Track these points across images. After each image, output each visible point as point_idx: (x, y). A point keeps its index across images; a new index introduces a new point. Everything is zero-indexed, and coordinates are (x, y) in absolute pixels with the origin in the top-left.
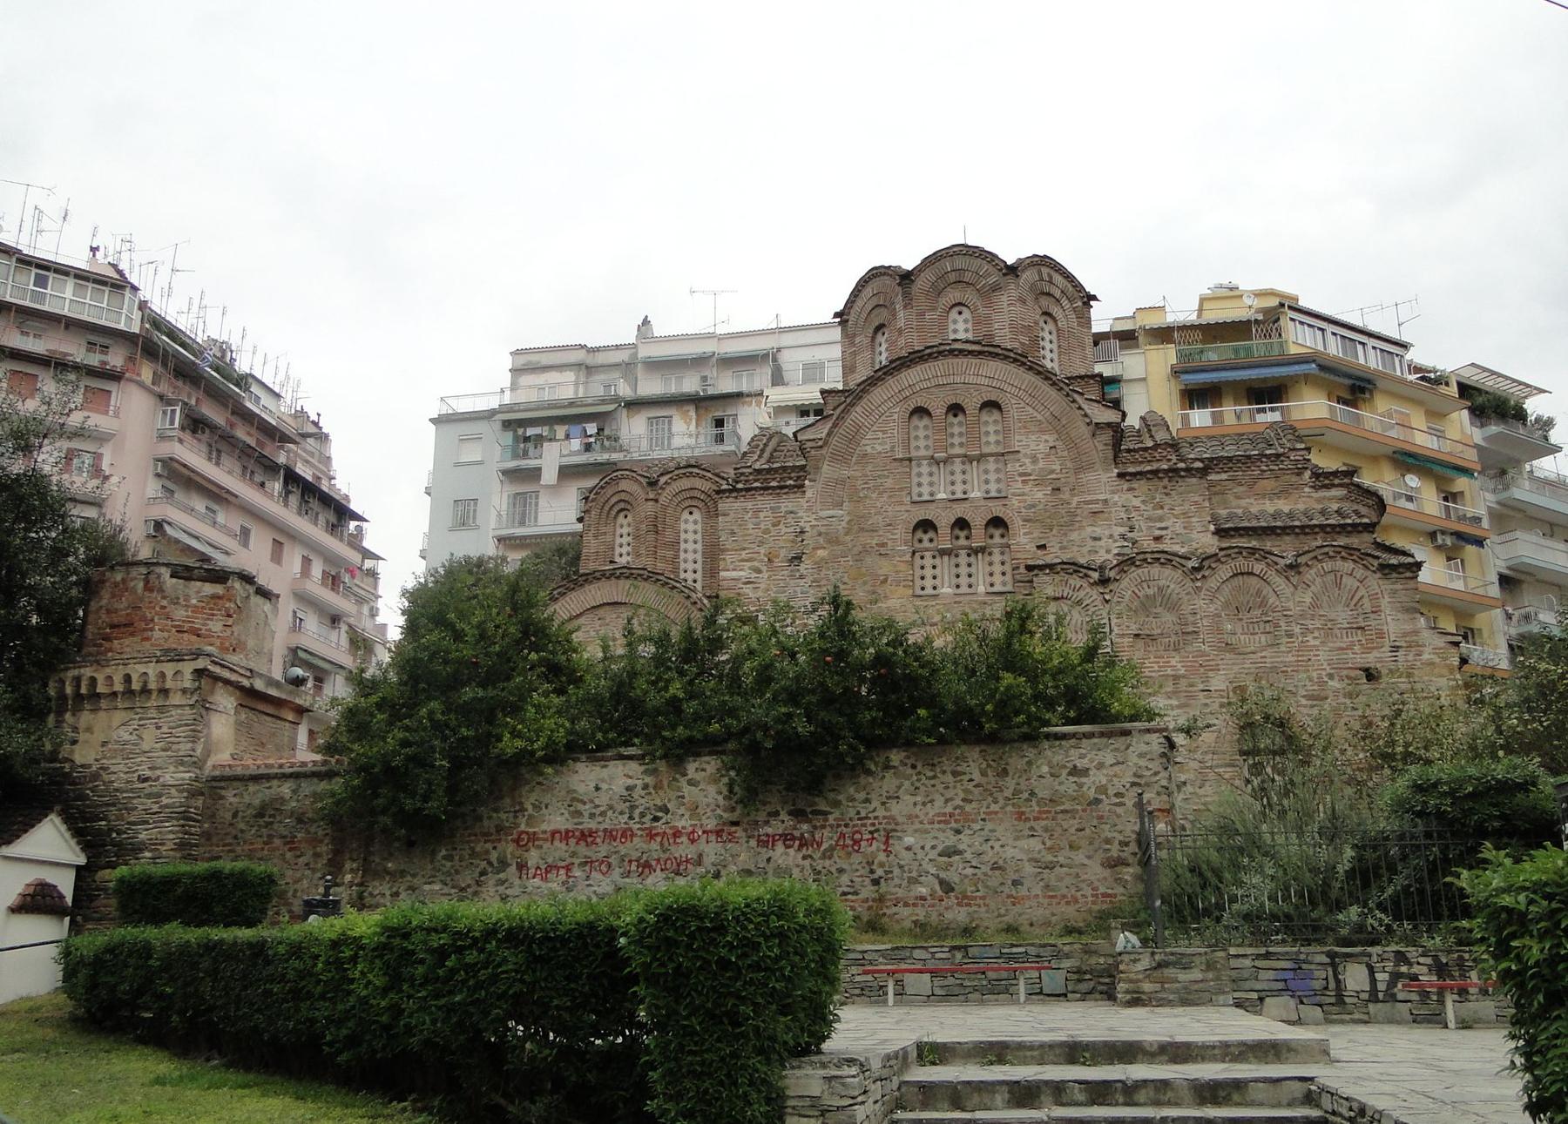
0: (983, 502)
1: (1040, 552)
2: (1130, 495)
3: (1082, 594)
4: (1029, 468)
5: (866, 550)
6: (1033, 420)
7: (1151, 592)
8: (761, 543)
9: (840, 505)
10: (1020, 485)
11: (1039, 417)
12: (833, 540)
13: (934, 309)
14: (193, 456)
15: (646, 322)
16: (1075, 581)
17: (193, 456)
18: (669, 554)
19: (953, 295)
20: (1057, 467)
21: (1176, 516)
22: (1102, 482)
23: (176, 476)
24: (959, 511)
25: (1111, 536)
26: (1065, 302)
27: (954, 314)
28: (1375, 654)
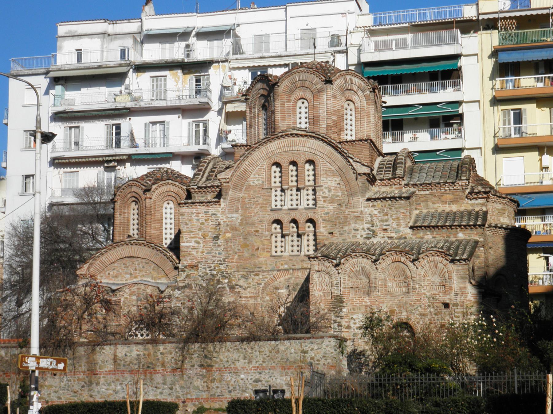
0: (304, 211)
1: (330, 236)
2: (373, 209)
3: (329, 269)
4: (327, 194)
5: (249, 233)
6: (330, 170)
7: (358, 269)
8: (200, 229)
9: (237, 211)
10: (322, 202)
11: (333, 168)
12: (234, 229)
13: (289, 101)
16: (327, 264)
18: (157, 225)
19: (299, 93)
20: (340, 194)
21: (393, 219)
24: (293, 215)
25: (363, 229)
26: (360, 93)
27: (299, 103)
28: (448, 297)
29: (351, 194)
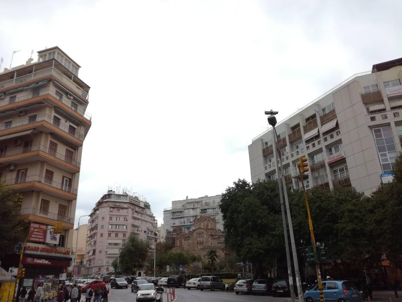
14: (136, 215)
15: (187, 197)
17: (136, 215)
19: (202, 221)
22: (210, 239)
23: (134, 218)
29: (209, 238)
